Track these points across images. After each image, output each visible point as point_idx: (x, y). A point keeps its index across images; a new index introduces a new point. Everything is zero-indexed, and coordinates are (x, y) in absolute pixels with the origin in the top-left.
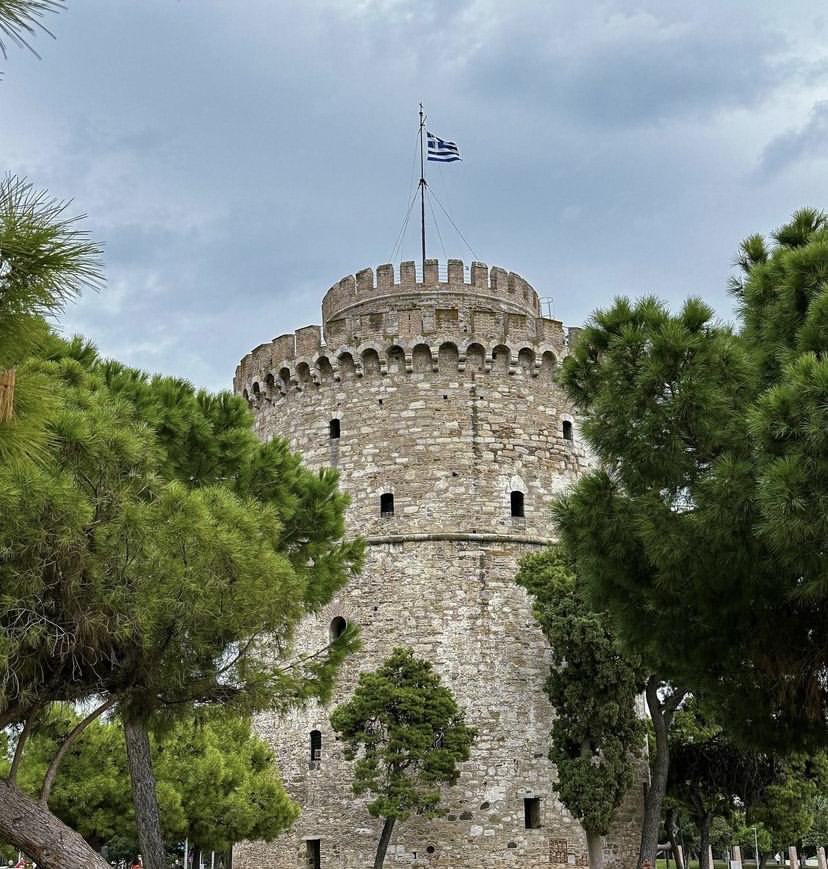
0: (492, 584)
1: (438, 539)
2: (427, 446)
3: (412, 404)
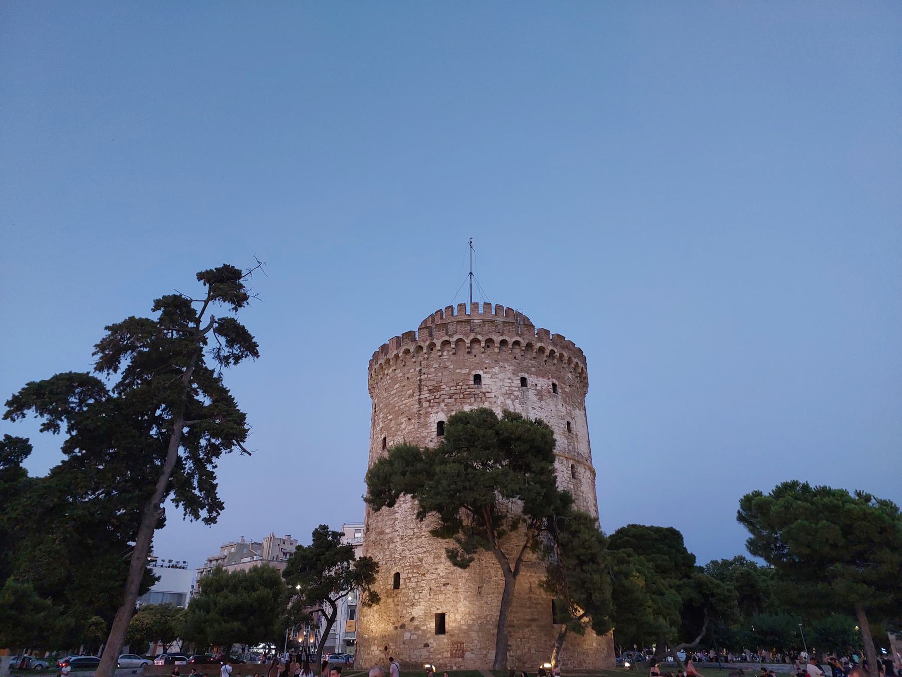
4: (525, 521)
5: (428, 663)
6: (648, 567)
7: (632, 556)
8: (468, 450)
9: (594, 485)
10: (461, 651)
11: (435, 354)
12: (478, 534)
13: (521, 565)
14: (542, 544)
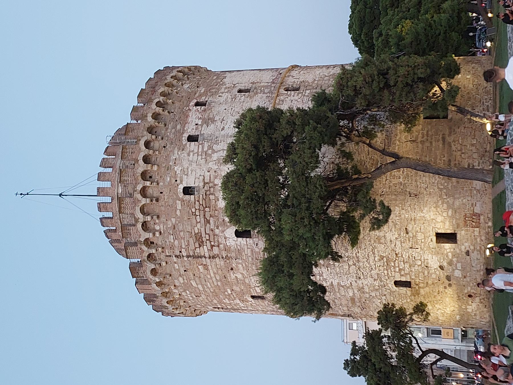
4: (343, 144)
5: (485, 252)
6: (393, 16)
7: (381, 31)
8: (267, 203)
9: (307, 67)
10: (474, 217)
11: (158, 239)
12: (356, 195)
13: (388, 150)
14: (366, 127)
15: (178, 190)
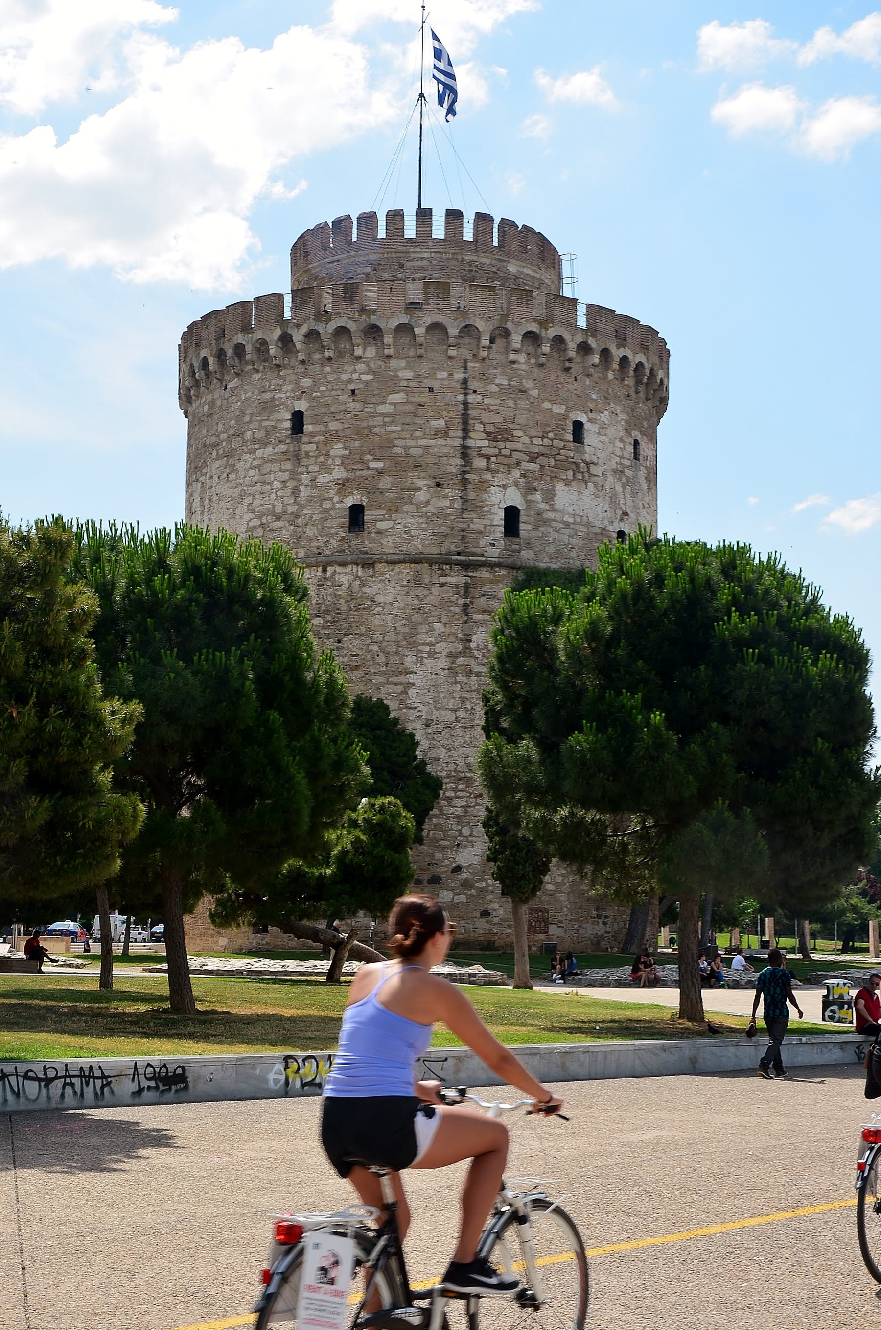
0: (477, 617)
1: (416, 560)
2: (406, 448)
3: (391, 396)
15: (579, 412)
